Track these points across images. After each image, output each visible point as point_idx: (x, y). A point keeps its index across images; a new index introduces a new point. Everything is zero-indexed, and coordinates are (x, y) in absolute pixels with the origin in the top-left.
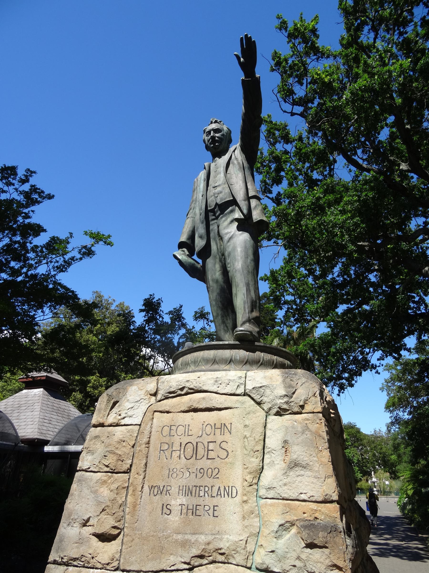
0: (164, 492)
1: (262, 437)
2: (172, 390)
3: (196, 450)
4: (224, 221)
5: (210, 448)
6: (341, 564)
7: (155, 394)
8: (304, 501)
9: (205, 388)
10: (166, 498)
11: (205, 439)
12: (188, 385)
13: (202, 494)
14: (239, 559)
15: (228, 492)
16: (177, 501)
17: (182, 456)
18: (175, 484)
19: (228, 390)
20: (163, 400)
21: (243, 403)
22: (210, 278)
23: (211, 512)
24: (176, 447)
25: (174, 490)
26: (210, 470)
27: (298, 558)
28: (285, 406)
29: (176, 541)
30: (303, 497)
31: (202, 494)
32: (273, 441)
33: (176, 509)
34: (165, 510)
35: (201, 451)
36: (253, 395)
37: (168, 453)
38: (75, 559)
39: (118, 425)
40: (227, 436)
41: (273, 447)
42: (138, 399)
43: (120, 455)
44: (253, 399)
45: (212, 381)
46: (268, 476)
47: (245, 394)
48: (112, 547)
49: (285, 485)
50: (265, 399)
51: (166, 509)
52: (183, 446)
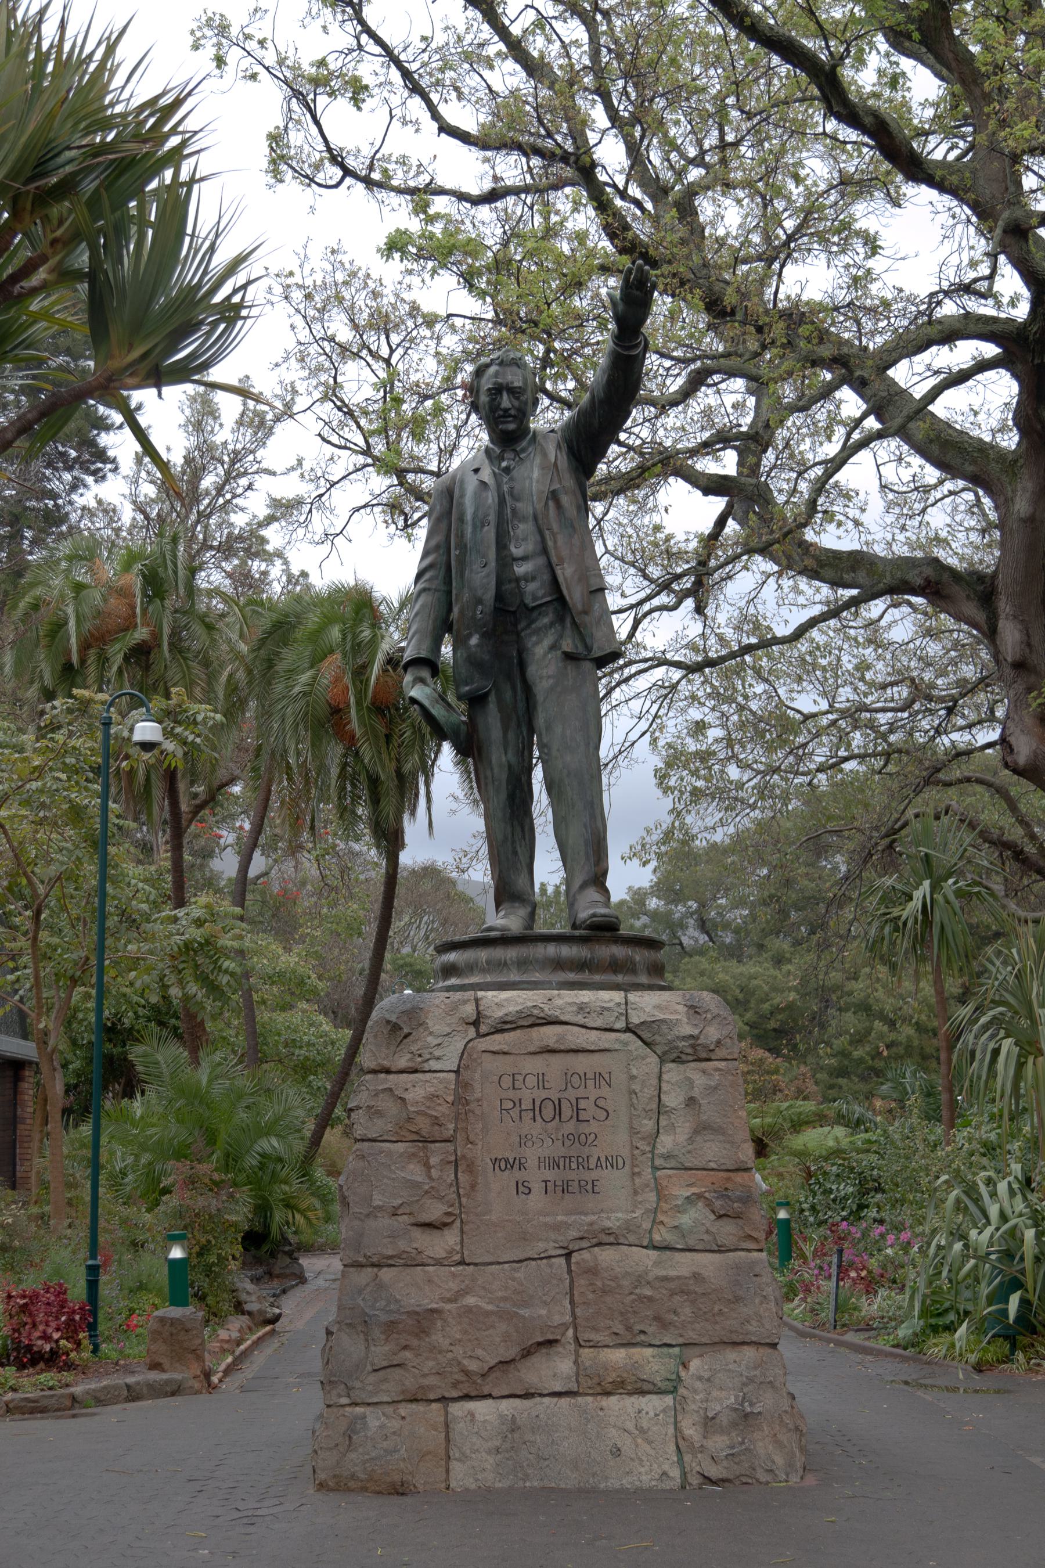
0: (516, 1166)
1: (656, 1093)
2: (509, 1019)
3: (558, 1110)
4: (537, 643)
5: (581, 1106)
6: (755, 1234)
7: (476, 1023)
8: (713, 1170)
9: (563, 1018)
10: (518, 1175)
11: (571, 1094)
12: (536, 1012)
13: (574, 1166)
14: (632, 1239)
15: (612, 1163)
16: (535, 1176)
17: (538, 1118)
18: (531, 1155)
19: (599, 1023)
20: (492, 1033)
21: (626, 1044)
22: (494, 761)
23: (589, 1187)
24: (527, 1105)
25: (532, 1162)
26: (583, 1137)
27: (707, 1232)
28: (689, 1050)
29: (546, 1224)
30: (713, 1165)
31: (574, 1166)
32: (673, 1099)
33: (537, 1187)
34: (521, 1188)
35: (567, 1111)
36: (640, 1033)
37: (515, 1113)
38: (391, 1257)
39: (416, 1071)
40: (605, 1091)
41: (672, 1105)
42: (448, 1030)
43: (436, 1118)
44: (639, 1037)
45: (575, 1009)
46: (666, 1142)
47: (628, 1029)
48: (450, 1238)
49: (689, 1152)
50: (657, 1038)
51: (523, 1188)
52: (537, 1104)
